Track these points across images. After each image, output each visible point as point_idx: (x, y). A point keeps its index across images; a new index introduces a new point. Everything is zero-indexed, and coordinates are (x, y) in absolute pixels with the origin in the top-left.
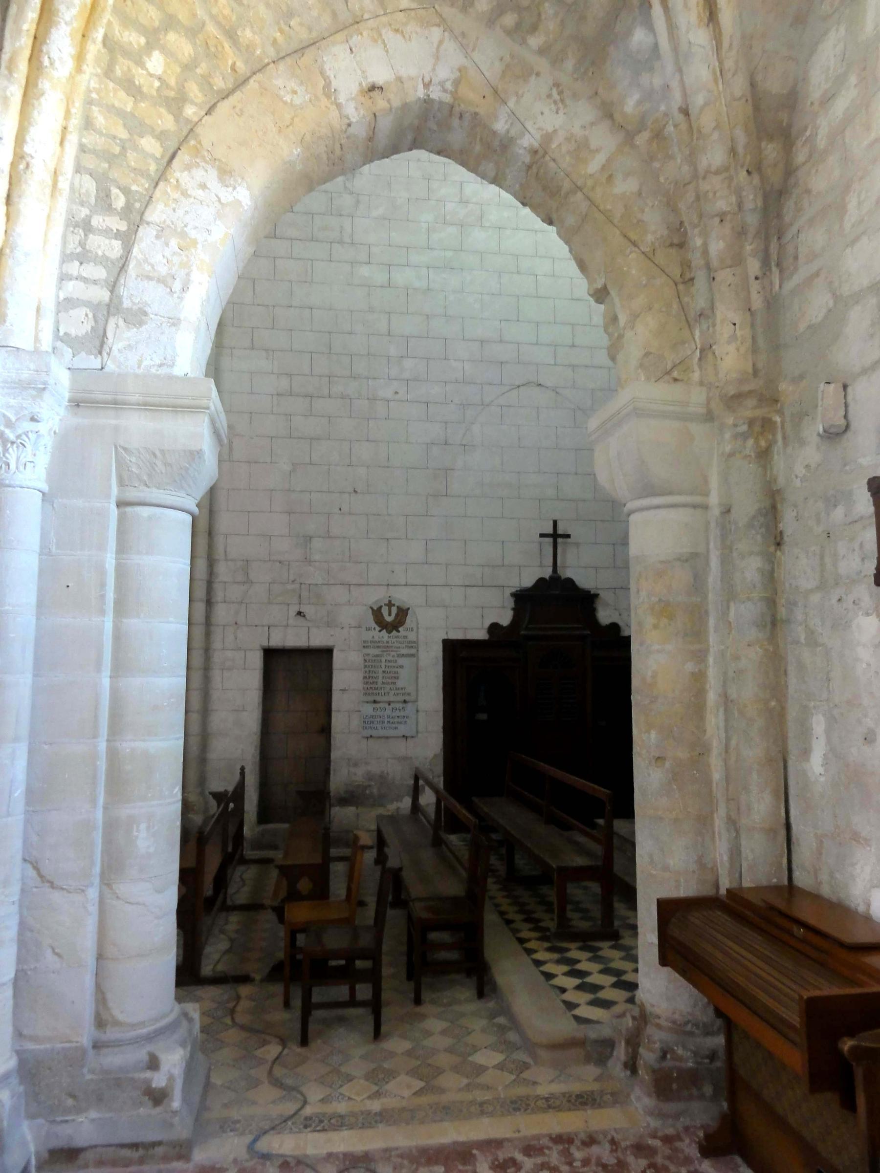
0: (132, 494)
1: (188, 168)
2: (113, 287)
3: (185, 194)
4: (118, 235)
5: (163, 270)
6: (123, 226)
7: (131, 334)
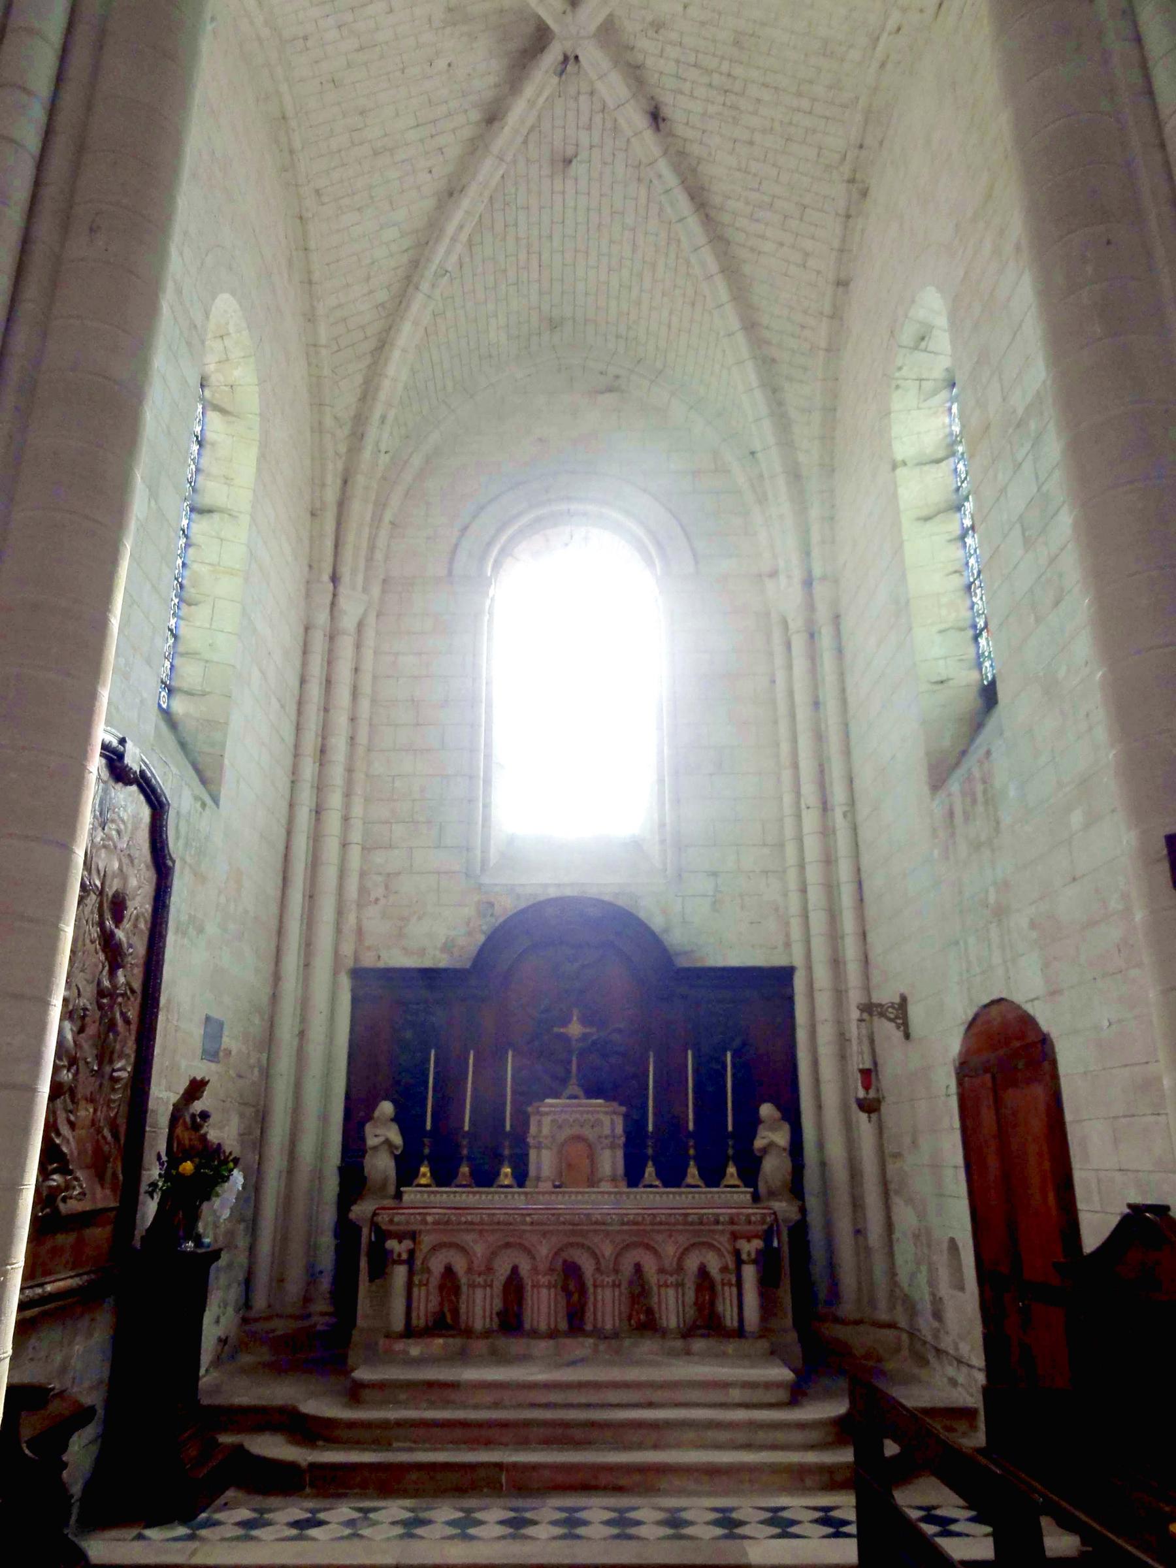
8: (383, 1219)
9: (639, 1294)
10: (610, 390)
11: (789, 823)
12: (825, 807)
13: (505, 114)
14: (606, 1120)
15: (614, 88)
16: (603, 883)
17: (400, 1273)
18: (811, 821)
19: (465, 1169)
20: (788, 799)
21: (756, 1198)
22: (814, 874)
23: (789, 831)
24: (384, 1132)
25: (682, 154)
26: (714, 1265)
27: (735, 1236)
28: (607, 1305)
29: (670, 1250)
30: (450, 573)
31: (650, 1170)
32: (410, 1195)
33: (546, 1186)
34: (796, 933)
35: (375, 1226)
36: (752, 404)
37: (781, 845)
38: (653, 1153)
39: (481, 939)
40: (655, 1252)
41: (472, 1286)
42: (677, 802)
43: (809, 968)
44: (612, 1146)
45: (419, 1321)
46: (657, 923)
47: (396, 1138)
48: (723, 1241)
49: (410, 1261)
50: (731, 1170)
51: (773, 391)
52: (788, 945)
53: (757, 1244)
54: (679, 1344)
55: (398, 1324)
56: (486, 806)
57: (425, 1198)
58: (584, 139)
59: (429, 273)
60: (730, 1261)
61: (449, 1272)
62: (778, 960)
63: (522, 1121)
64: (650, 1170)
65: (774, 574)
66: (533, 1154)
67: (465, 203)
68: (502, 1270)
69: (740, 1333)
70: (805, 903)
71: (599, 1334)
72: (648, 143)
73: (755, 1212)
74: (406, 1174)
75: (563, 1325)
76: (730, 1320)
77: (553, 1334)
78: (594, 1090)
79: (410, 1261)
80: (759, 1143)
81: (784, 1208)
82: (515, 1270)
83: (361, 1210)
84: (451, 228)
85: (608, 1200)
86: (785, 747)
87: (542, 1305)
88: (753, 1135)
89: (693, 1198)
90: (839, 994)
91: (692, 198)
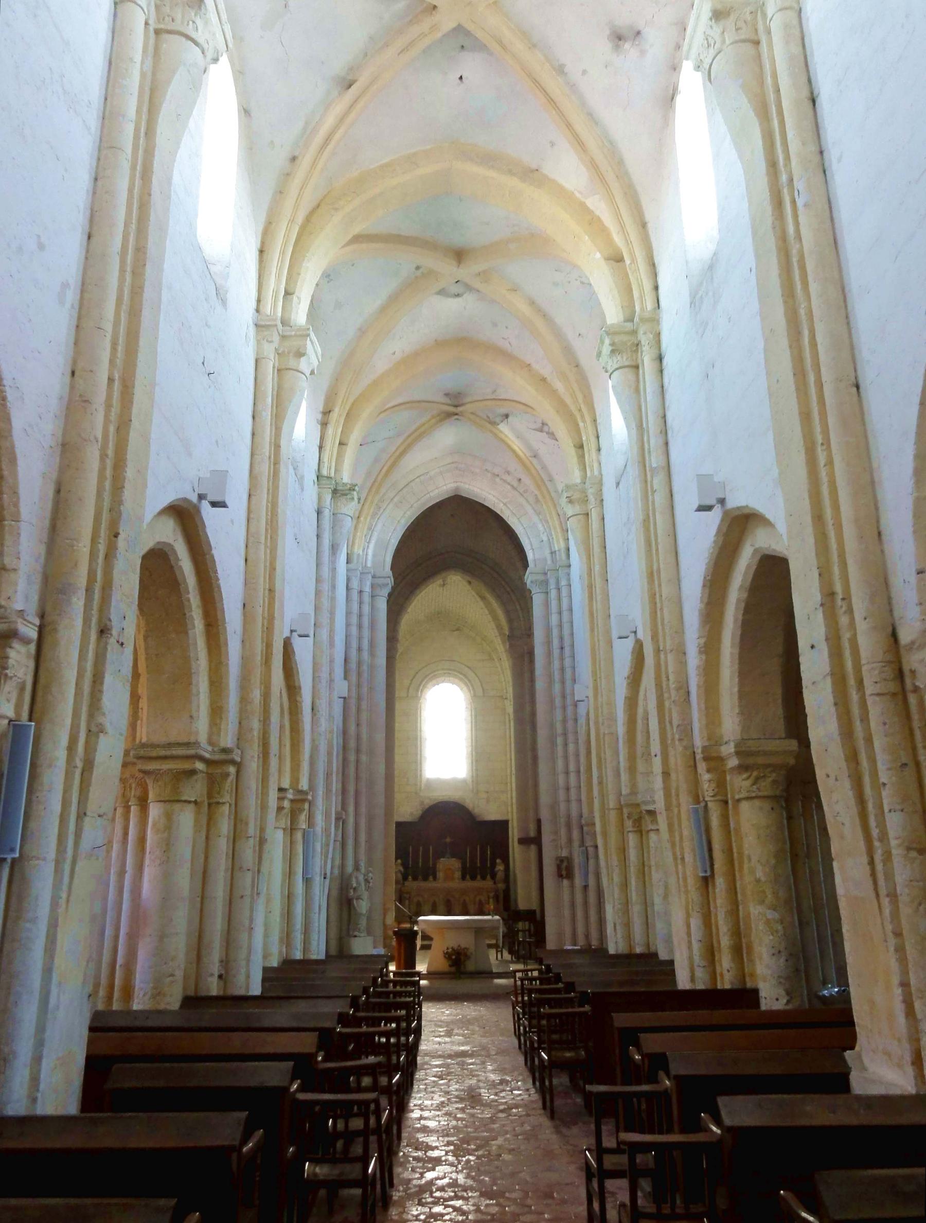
10: (457, 630)
17: (407, 902)
20: (509, 771)
21: (495, 883)
31: (468, 877)
32: (407, 883)
34: (510, 809)
38: (469, 872)
39: (420, 812)
42: (477, 770)
57: (411, 884)
62: (504, 818)
64: (468, 877)
74: (405, 878)
78: (453, 856)
80: (496, 869)
85: (456, 884)
87: (441, 908)
88: (495, 867)
89: (478, 883)
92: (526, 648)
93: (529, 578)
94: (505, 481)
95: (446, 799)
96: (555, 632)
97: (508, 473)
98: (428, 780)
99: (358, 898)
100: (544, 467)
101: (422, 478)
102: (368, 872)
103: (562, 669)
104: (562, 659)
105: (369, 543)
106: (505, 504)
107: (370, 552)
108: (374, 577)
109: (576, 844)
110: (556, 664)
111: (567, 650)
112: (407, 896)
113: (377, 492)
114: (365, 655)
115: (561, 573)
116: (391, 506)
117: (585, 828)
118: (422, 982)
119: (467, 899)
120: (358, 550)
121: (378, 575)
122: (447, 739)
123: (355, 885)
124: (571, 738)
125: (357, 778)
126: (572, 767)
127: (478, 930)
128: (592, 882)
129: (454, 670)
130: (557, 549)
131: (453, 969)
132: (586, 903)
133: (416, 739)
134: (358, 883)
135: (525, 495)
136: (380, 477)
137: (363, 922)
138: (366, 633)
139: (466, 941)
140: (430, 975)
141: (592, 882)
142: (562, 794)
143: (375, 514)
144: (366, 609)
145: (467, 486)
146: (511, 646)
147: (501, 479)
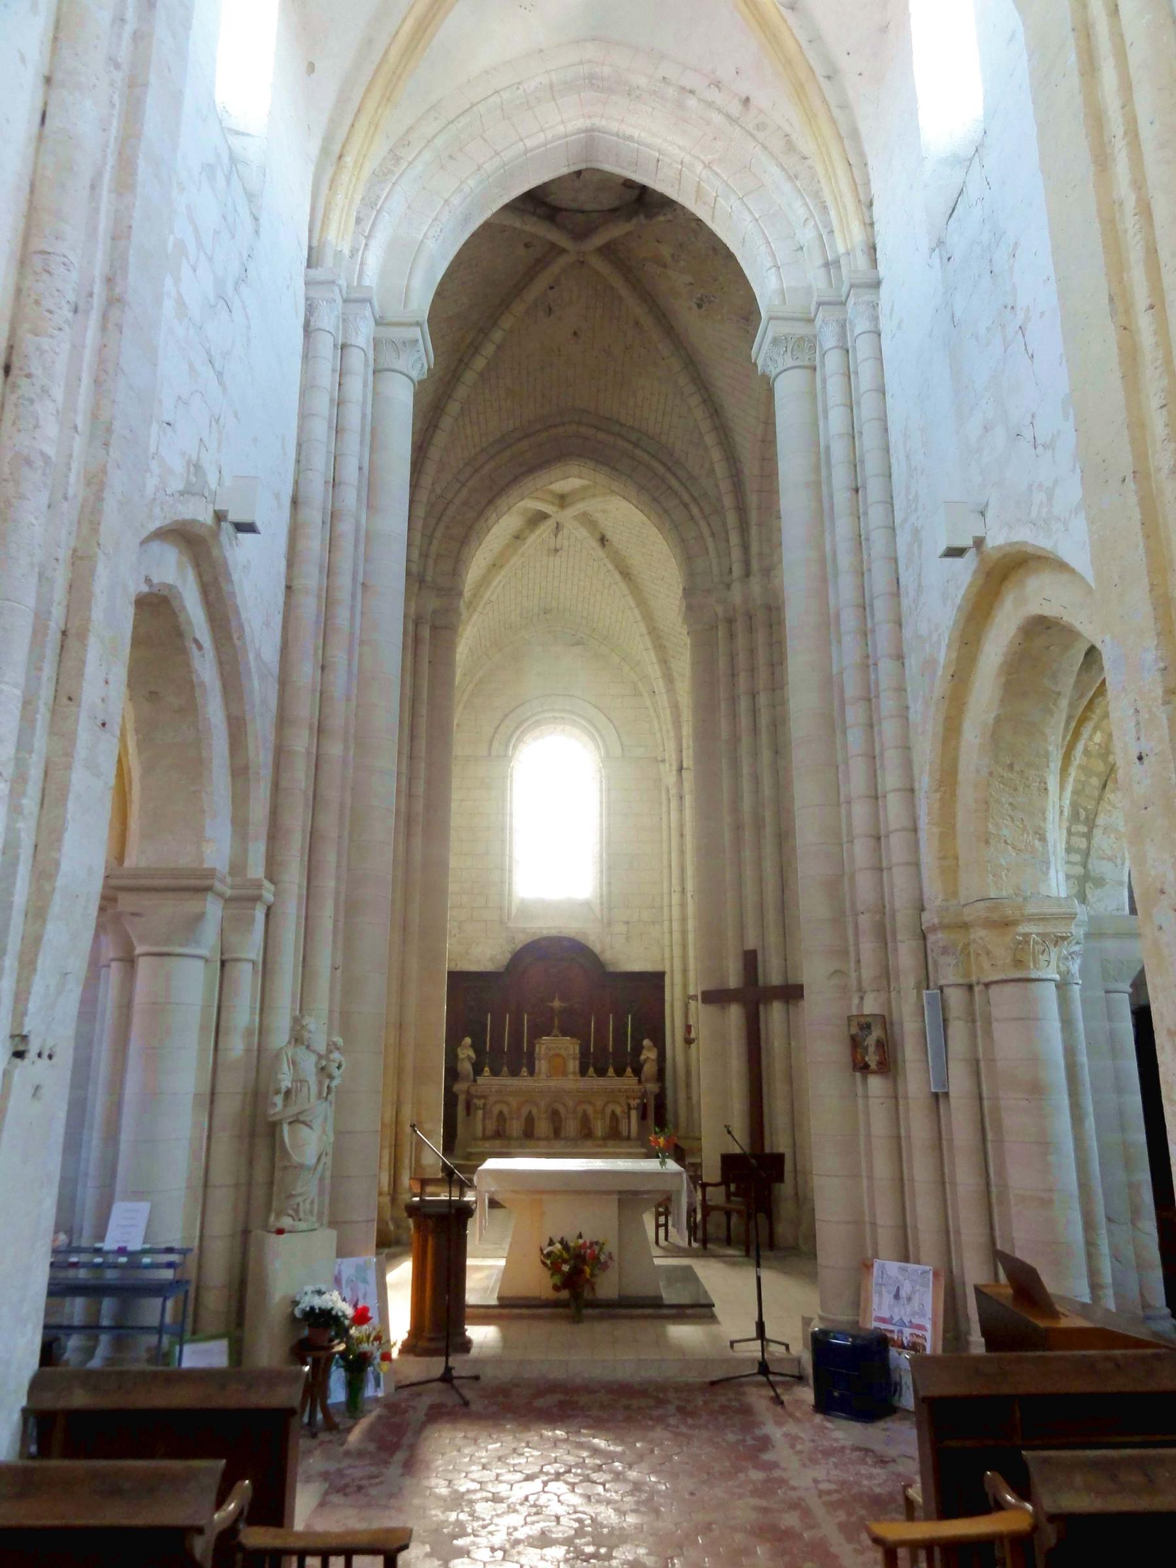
0: (1112, 986)
1: (1113, 791)
2: (1085, 866)
3: (1114, 806)
4: (1083, 835)
5: (1109, 853)
6: (1085, 829)
7: (1098, 892)
8: (473, 1090)
9: (585, 1121)
10: (578, 643)
11: (666, 897)
12: (683, 891)
13: (525, 539)
14: (571, 1047)
15: (582, 533)
16: (570, 927)
17: (480, 1112)
18: (676, 898)
19: (505, 1069)
20: (666, 885)
21: (640, 1082)
22: (676, 926)
23: (666, 902)
24: (466, 1052)
25: (617, 552)
26: (618, 1111)
27: (628, 1097)
28: (571, 1127)
29: (599, 1103)
30: (490, 755)
31: (591, 1069)
32: (480, 1080)
33: (543, 1076)
34: (667, 955)
35: (468, 1093)
36: (654, 670)
37: (662, 908)
38: (592, 1062)
39: (509, 956)
40: (593, 1105)
41: (512, 1119)
42: (609, 884)
43: (672, 971)
44: (574, 1059)
45: (489, 1132)
46: (597, 949)
47: (472, 1054)
48: (623, 1101)
49: (484, 1108)
50: (629, 1070)
51: (664, 662)
52: (663, 959)
53: (638, 1101)
54: (601, 1142)
55: (479, 1134)
56: (510, 884)
57: (486, 1080)
58: (566, 543)
59: (481, 605)
60: (625, 1107)
61: (501, 1113)
63: (532, 1046)
64: (591, 1069)
65: (663, 761)
66: (537, 1063)
67: (503, 573)
68: (525, 1112)
69: (628, 1138)
70: (671, 941)
71: (566, 1139)
72: (600, 552)
73: (637, 1088)
74: (478, 1070)
75: (552, 1136)
76: (625, 1133)
77: (547, 1139)
79: (484, 1108)
80: (643, 1057)
81: (652, 1087)
82: (530, 1112)
83: (460, 1087)
84: (495, 583)
85: (572, 1082)
86: (665, 857)
87: (543, 1126)
88: (640, 1053)
89: (611, 1082)
90: (685, 986)
91: (621, 573)
92: (719, 609)
93: (764, 351)
94: (710, 105)
95: (554, 933)
96: (839, 451)
97: (718, 85)
98: (523, 901)
99: (295, 1121)
100: (816, 39)
101: (506, 95)
102: (332, 1047)
103: (859, 542)
104: (857, 516)
105: (368, 238)
106: (708, 166)
107: (374, 259)
108: (379, 322)
109: (908, 982)
110: (843, 526)
111: (874, 490)
112: (480, 1102)
113: (387, 98)
114: (350, 497)
115: (856, 311)
116: (427, 155)
117: (931, 938)
118: (481, 1335)
119: (590, 1110)
120: (339, 238)
121: (391, 316)
122: (561, 828)
123: (286, 1082)
124: (887, 704)
125: (316, 800)
126: (891, 779)
127: (628, 1197)
128: (959, 1083)
129: (572, 712)
130: (841, 249)
131: (565, 1294)
132: (939, 1143)
133: (503, 829)
134: (300, 1081)
135: (760, 136)
136: (393, 57)
137: (308, 1190)
138: (353, 444)
139: (591, 1224)
140: (509, 1308)
141: (959, 1083)
142: (861, 851)
143: (381, 175)
144: (356, 387)
145: (614, 126)
146: (690, 608)
147: (700, 100)
